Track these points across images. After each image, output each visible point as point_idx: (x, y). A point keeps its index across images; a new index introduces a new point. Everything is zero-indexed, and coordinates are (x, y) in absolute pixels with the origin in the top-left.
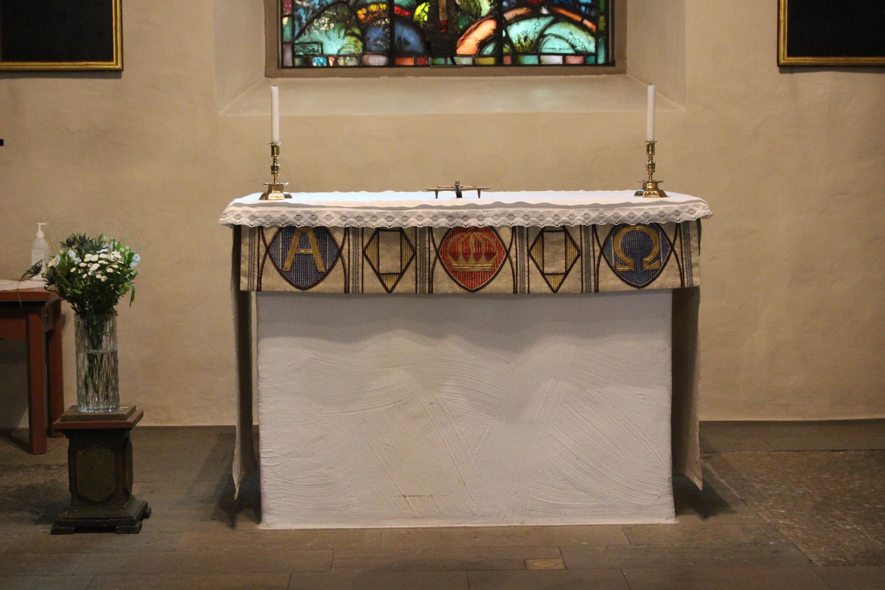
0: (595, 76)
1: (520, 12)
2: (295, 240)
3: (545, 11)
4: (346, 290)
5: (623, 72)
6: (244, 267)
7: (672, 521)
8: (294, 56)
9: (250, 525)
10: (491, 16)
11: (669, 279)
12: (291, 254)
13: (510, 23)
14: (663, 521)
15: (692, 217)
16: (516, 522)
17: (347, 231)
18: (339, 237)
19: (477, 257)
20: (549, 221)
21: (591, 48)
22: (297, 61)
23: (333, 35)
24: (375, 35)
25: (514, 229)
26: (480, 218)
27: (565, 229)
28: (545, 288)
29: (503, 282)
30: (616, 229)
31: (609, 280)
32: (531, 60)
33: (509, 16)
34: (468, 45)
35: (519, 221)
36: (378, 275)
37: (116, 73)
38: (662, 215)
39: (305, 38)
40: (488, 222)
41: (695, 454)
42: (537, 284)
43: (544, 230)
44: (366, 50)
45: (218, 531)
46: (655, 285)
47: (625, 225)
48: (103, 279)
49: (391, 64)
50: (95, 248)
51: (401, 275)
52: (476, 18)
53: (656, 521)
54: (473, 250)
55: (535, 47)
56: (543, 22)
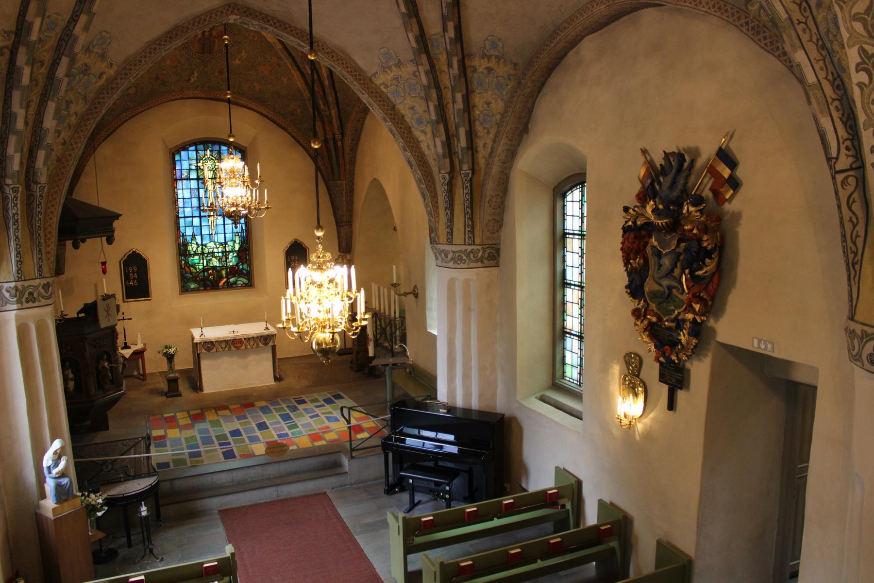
9: (200, 392)
10: (225, 277)
11: (271, 344)
16: (248, 387)
20: (250, 336)
24: (201, 283)
29: (243, 347)
30: (262, 337)
31: (261, 345)
32: (234, 286)
34: (221, 283)
35: (245, 337)
37: (150, 300)
41: (277, 370)
42: (249, 347)
45: (195, 394)
50: (170, 348)
52: (221, 278)
55: (235, 283)
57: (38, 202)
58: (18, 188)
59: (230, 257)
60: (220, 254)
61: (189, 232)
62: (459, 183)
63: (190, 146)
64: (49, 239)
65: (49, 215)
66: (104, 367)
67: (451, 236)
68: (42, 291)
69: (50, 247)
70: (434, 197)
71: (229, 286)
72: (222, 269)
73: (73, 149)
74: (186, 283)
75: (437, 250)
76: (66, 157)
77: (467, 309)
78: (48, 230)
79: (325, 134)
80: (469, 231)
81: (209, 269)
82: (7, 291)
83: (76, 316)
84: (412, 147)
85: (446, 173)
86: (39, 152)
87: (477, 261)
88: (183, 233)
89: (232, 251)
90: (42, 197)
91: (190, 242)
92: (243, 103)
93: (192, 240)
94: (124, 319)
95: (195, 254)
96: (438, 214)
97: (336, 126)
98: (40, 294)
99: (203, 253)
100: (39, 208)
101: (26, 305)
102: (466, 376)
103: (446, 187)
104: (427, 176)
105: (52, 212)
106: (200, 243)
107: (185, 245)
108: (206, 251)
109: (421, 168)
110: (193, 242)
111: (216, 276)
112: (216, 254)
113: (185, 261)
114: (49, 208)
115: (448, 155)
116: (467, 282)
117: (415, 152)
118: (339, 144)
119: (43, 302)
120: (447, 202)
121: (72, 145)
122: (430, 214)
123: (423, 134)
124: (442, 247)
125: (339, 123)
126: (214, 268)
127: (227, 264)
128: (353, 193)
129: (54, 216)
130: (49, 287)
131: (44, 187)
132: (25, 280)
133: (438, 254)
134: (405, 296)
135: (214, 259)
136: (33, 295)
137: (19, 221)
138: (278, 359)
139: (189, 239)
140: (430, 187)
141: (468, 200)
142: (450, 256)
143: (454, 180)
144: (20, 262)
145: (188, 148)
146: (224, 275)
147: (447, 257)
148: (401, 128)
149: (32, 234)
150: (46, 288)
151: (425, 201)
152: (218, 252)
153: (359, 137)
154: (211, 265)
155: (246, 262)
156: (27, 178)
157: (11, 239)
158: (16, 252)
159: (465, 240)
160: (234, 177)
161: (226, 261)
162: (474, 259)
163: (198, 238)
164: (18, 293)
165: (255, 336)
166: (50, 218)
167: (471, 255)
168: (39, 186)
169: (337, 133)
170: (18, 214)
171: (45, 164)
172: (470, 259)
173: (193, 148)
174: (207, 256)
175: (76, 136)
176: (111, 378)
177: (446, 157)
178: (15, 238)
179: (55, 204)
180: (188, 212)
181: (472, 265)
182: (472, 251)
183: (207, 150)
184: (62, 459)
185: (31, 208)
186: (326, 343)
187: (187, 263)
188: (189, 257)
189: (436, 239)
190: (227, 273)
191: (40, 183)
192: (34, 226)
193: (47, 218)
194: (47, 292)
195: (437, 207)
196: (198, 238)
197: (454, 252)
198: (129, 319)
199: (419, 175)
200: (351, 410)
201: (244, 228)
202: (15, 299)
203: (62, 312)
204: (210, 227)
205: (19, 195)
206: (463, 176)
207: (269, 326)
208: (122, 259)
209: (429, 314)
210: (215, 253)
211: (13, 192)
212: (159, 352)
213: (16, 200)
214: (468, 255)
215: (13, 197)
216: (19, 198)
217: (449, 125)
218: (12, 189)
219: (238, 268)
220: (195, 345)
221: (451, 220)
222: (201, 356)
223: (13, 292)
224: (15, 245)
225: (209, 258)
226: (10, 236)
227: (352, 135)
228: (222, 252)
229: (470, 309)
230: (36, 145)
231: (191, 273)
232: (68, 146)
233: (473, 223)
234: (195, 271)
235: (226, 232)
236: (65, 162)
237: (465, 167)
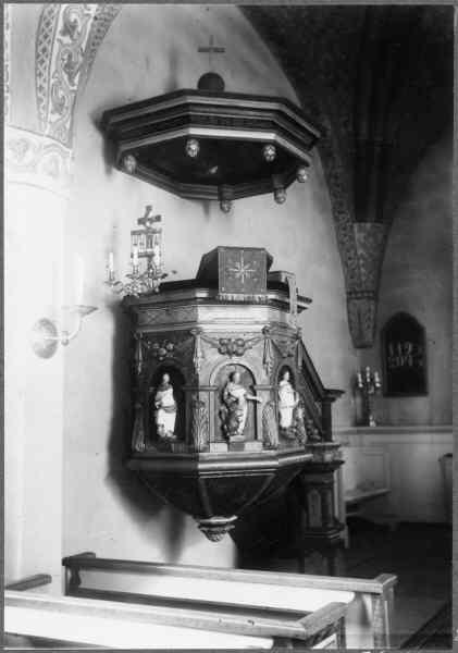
64: (43, 61)
78: (40, 48)
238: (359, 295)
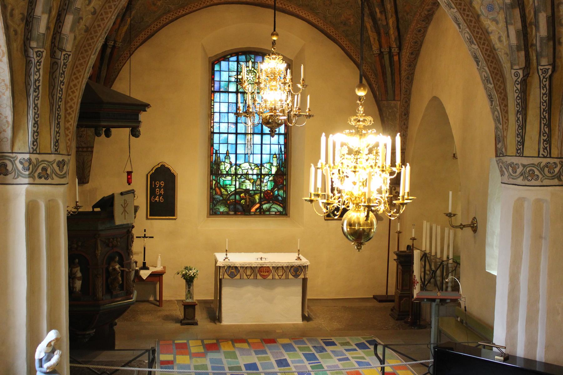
0: (283, 218)
1: (265, 202)
2: (231, 269)
3: (271, 202)
4: (240, 278)
5: (289, 217)
6: (221, 274)
7: (302, 323)
8: (212, 212)
9: (218, 324)
10: (258, 203)
11: (302, 276)
12: (230, 271)
13: (263, 205)
14: (300, 323)
15: (307, 265)
16: (271, 323)
17: (241, 267)
18: (239, 268)
19: (266, 272)
20: (279, 265)
21: (282, 210)
22: (213, 213)
23: (222, 207)
24: (232, 207)
25: (273, 267)
26: (266, 265)
27: (282, 267)
28: (278, 278)
30: (292, 267)
31: (290, 276)
32: (267, 213)
33: (263, 203)
34: (253, 209)
35: (274, 265)
36: (246, 275)
37: (175, 219)
38: (301, 264)
39: (216, 208)
40: (268, 266)
41: (306, 309)
42: (277, 277)
43: (278, 267)
44: (229, 210)
46: (299, 277)
47: (294, 266)
48: (193, 276)
49: (235, 214)
50: (191, 269)
51: (251, 275)
52: (254, 203)
53: (298, 323)
54: (265, 271)
55: (269, 210)
56: (271, 204)
57: (61, 71)
58: (42, 52)
59: (265, 181)
60: (255, 177)
61: (223, 149)
62: (535, 82)
63: (232, 56)
64: (69, 114)
65: (71, 88)
66: (114, 269)
67: (521, 146)
68: (57, 169)
69: (70, 123)
70: (503, 99)
71: (262, 212)
72: (255, 194)
73: (103, 19)
74: (215, 205)
75: (503, 163)
76: (94, 27)
77: (538, 237)
78: (69, 105)
79: (381, 46)
80: (544, 141)
81: (241, 192)
82: (21, 163)
83: (91, 210)
84: (480, 38)
85: (520, 69)
86: (67, 16)
87: (553, 178)
88: (216, 151)
89: (268, 175)
90: (66, 65)
91: (224, 160)
92: (291, 10)
93: (225, 158)
94: (145, 237)
95: (228, 174)
96: (507, 120)
97: (393, 37)
98: (53, 171)
99: (236, 174)
100: (62, 77)
101: (38, 181)
102: (531, 320)
103: (519, 87)
104: (497, 74)
105: (75, 85)
106: (234, 162)
107: (218, 163)
108: (240, 171)
109: (489, 64)
110: (226, 161)
111: (248, 200)
112: (250, 176)
113: (216, 182)
114: (73, 81)
115: (523, 47)
116: (538, 202)
117: (484, 44)
118: (396, 58)
119: (57, 180)
120: (518, 104)
121: (102, 14)
122: (497, 120)
123: (494, 23)
124: (509, 160)
125: (396, 34)
126: (247, 191)
127: (261, 188)
128: (408, 117)
129: (77, 90)
130: (64, 165)
131: (69, 55)
132: (39, 154)
133: (504, 169)
134: (462, 229)
135: (247, 181)
136: (46, 170)
137: (40, 88)
138: (308, 299)
139: (222, 157)
140: (500, 87)
141: (545, 102)
142: (519, 171)
143: (529, 78)
144: (36, 133)
145: (228, 58)
146: (257, 201)
147: (516, 172)
148: (468, 15)
149: (52, 105)
150: (61, 165)
151: (492, 105)
152: (253, 175)
153: (419, 50)
154: (244, 188)
155: (282, 188)
156: (53, 44)
157: (30, 108)
158: (34, 122)
159: (539, 152)
160: (275, 79)
161: (261, 185)
162: (550, 175)
163: (233, 157)
164: (31, 166)
165: (285, 265)
166: (72, 92)
167: (546, 170)
168: (64, 53)
169: (394, 45)
170: (39, 81)
171: (72, 30)
172: (544, 175)
173: (234, 58)
174: (240, 178)
175: (107, 6)
176: (121, 282)
177: (522, 50)
178: (34, 106)
179: (79, 77)
180: (224, 128)
181: (546, 182)
182: (547, 165)
183: (249, 61)
184: (55, 353)
185: (54, 77)
186: (359, 224)
187: (218, 183)
188: (221, 177)
189: (504, 150)
190: (260, 198)
191: (65, 51)
192: (55, 97)
193: (69, 91)
194: (61, 170)
195: (507, 112)
196: (233, 157)
197: (524, 166)
198: (150, 237)
199: (486, 72)
200: (386, 348)
201: (283, 150)
202: (27, 173)
203: (77, 202)
204: (246, 146)
205: (42, 60)
206: (540, 72)
207: (300, 256)
208: (149, 172)
209: (488, 250)
210: (249, 174)
211: (37, 56)
212: (178, 273)
213: (39, 65)
214: (542, 170)
215: (36, 61)
216: (42, 64)
217: (527, 11)
218: (37, 52)
219: (274, 193)
220: (218, 269)
221: (523, 127)
222: (223, 281)
223: (27, 165)
224: (34, 114)
225: (242, 180)
226: (29, 104)
227: (411, 47)
228: (257, 175)
229: (541, 237)
230: (64, 10)
231: (222, 195)
232: (97, 16)
233: (550, 130)
234: (226, 193)
235: (263, 153)
236: (93, 33)
237: (544, 61)
238: (85, 150)
